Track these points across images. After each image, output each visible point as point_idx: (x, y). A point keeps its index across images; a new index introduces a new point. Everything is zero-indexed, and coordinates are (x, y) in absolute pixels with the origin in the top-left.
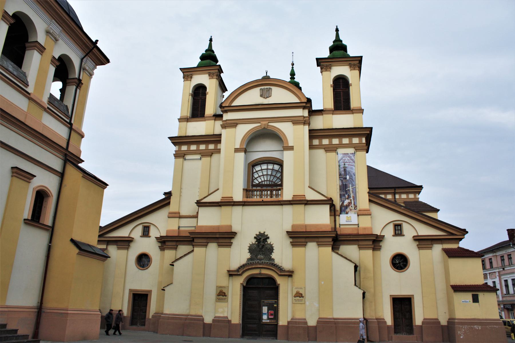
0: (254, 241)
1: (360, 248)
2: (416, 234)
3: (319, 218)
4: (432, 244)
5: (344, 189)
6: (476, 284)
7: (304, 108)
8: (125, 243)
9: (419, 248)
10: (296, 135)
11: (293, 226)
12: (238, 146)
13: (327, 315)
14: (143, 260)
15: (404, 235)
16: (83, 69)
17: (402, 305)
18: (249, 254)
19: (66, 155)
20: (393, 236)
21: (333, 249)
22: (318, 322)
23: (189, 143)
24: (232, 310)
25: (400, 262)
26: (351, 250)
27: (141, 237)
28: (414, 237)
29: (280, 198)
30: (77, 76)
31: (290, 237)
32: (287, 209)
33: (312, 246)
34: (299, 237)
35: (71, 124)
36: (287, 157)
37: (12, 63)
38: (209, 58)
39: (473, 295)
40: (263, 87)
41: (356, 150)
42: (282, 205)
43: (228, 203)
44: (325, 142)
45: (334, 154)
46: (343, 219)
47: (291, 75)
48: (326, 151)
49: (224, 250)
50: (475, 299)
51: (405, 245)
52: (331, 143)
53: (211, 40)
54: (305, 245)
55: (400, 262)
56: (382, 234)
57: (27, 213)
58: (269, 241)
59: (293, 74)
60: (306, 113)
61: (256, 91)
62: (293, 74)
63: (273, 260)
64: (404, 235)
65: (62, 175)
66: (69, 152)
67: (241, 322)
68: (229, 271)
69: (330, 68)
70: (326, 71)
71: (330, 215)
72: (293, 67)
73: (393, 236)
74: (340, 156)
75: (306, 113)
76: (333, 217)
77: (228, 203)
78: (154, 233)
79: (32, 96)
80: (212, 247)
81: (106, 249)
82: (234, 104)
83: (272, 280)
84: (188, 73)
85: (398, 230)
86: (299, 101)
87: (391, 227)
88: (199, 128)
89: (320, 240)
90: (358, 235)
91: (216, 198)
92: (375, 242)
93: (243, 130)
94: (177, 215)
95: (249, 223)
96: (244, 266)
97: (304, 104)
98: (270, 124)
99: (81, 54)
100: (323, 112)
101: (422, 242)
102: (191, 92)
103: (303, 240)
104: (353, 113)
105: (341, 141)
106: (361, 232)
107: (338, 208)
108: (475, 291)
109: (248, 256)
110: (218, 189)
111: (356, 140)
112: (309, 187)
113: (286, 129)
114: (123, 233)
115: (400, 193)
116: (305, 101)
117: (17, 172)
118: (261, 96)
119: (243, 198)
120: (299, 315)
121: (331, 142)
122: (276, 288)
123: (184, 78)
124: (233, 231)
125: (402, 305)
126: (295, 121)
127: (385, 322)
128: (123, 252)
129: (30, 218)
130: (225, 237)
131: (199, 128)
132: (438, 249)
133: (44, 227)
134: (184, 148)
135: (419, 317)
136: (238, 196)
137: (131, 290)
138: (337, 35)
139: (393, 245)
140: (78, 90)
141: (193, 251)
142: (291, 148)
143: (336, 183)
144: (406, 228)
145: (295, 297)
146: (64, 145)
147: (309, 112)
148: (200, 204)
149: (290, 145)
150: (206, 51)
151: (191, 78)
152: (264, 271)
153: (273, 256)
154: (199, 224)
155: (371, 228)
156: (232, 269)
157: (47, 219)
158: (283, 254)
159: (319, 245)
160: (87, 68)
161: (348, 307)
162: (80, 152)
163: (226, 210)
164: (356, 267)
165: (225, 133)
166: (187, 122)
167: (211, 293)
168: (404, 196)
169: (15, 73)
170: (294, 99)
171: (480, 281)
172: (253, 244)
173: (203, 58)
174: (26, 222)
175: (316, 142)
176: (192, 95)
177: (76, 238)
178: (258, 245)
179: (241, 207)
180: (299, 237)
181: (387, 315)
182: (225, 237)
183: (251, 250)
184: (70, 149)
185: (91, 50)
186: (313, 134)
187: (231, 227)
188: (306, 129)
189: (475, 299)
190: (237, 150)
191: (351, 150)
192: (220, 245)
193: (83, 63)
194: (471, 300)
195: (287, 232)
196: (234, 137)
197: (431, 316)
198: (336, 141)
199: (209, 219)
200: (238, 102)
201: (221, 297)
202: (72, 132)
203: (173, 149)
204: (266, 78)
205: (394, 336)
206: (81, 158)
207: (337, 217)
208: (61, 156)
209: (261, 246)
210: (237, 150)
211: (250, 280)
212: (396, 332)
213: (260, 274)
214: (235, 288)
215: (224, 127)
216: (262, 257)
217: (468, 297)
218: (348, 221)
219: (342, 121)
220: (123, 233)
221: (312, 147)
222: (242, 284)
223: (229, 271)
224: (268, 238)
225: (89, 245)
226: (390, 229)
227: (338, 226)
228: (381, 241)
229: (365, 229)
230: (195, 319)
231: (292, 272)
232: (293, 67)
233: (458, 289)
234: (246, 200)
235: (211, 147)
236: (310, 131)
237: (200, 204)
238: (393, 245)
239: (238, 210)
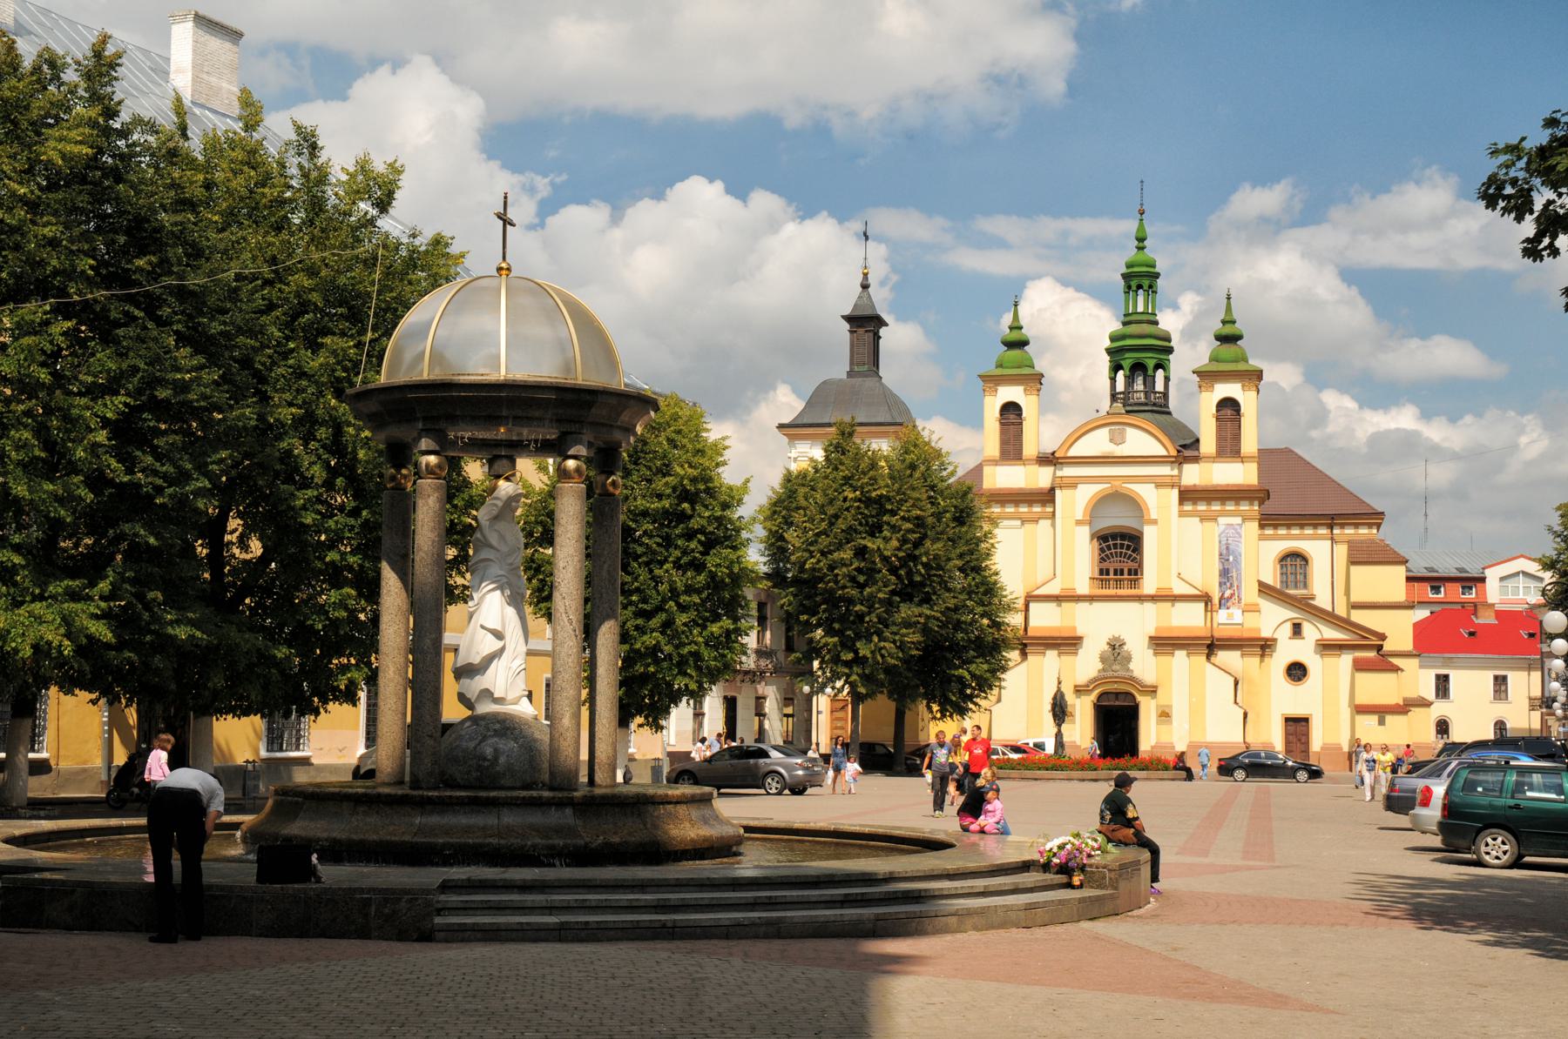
3: (1189, 618)
5: (1225, 573)
10: (1159, 502)
11: (1157, 629)
12: (1080, 517)
13: (1198, 738)
17: (1297, 726)
21: (1208, 657)
25: (1297, 671)
32: (1148, 606)
33: (1181, 655)
34: (1163, 643)
44: (1202, 507)
46: (1222, 616)
48: (1202, 520)
51: (1303, 650)
55: (1297, 671)
61: (1104, 433)
74: (1222, 528)
80: (1052, 654)
82: (1071, 453)
85: (1297, 630)
86: (1164, 453)
87: (1288, 626)
91: (1053, 589)
92: (1265, 647)
95: (1102, 623)
101: (1326, 647)
106: (1246, 635)
107: (1216, 600)
108: (1382, 712)
109: (1100, 666)
111: (1244, 507)
113: (1146, 492)
115: (1342, 526)
116: (1174, 453)
119: (1091, 587)
120: (1165, 739)
124: (1079, 634)
125: (1297, 726)
126: (1160, 483)
132: (1347, 659)
136: (1083, 588)
138: (1229, 309)
142: (1155, 522)
143: (1216, 567)
144: (1307, 628)
149: (1153, 516)
153: (1131, 666)
154: (1032, 623)
158: (1144, 665)
161: (1224, 730)
164: (1236, 683)
165: (1059, 495)
168: (1349, 531)
170: (1157, 449)
171: (1394, 699)
175: (1189, 507)
180: (1163, 643)
182: (1068, 643)
183: (1103, 659)
186: (1188, 495)
188: (1175, 492)
190: (1079, 523)
191: (1238, 520)
196: (1074, 503)
197: (1331, 740)
198: (1216, 507)
199: (1044, 618)
200: (1077, 450)
210: (1079, 523)
211: (1101, 696)
217: (1374, 718)
218: (1229, 619)
221: (1182, 514)
226: (1288, 628)
233: (1361, 710)
235: (1037, 509)
237: (1030, 598)
238: (1289, 650)
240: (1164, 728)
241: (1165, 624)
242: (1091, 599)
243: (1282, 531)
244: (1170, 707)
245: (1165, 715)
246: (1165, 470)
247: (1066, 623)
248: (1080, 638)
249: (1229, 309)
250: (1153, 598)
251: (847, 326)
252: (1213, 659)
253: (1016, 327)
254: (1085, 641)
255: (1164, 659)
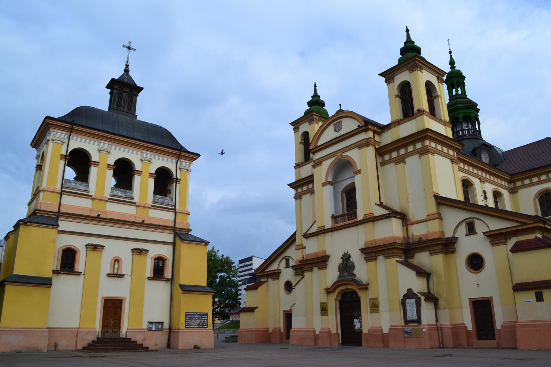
0: (341, 261)
1: (432, 254)
2: (488, 230)
4: (506, 239)
6: (545, 279)
7: (366, 130)
8: (276, 275)
9: (492, 244)
11: (365, 243)
14: (289, 287)
15: (476, 233)
16: (180, 169)
17: (482, 308)
18: (339, 273)
19: (174, 231)
20: (466, 235)
22: (390, 329)
23: (301, 186)
24: (332, 323)
25: (475, 262)
26: (422, 258)
27: (285, 268)
28: (484, 233)
29: (355, 220)
30: (175, 177)
31: (365, 254)
32: (361, 228)
34: (371, 252)
35: (175, 209)
36: (358, 179)
37: (122, 190)
38: (316, 103)
39: (536, 293)
40: (335, 123)
41: (420, 154)
42: (357, 225)
43: (323, 231)
44: (394, 155)
45: (402, 165)
47: (450, 64)
49: (322, 272)
50: (539, 298)
52: (399, 156)
53: (315, 86)
54: (375, 259)
55: (475, 262)
56: (456, 236)
57: (149, 272)
58: (351, 259)
59: (452, 63)
60: (370, 134)
62: (452, 63)
63: (355, 275)
64: (476, 233)
65: (174, 244)
66: (176, 228)
67: (339, 332)
68: (325, 289)
69: (393, 79)
70: (390, 83)
71: (403, 226)
72: (451, 56)
73: (466, 235)
75: (370, 134)
76: (405, 227)
77: (323, 231)
78: (292, 263)
79: (137, 204)
81: (267, 281)
83: (354, 294)
84: (296, 125)
88: (307, 170)
89: (386, 252)
90: (427, 241)
91: (314, 229)
92: (447, 246)
93: (326, 164)
94: (301, 247)
96: (335, 283)
97: (364, 128)
98: (344, 154)
99: (174, 160)
100: (390, 126)
101: (495, 238)
102: (300, 141)
103: (374, 255)
104: (415, 118)
105: (406, 150)
106: (430, 238)
108: (538, 288)
110: (315, 221)
111: (419, 145)
112: (381, 205)
113: (354, 154)
114: (274, 267)
116: (363, 124)
117: (136, 251)
118: (335, 130)
121: (398, 153)
122: (358, 300)
123: (294, 129)
125: (482, 308)
126: (360, 145)
127: (466, 328)
128: (276, 281)
129: (152, 276)
130: (321, 261)
131: (307, 170)
133: (167, 280)
134: (300, 190)
135: (499, 322)
136: (328, 224)
137: (284, 311)
139: (468, 245)
140: (178, 185)
141: (303, 276)
142: (359, 172)
145: (371, 307)
146: (172, 225)
147: (374, 132)
148: (307, 236)
150: (312, 97)
151: (298, 128)
152: (349, 287)
153: (355, 272)
155: (443, 233)
156: (329, 287)
157: (168, 274)
158: (362, 270)
159: (386, 257)
160: (182, 167)
162: (189, 225)
163: (321, 237)
166: (300, 167)
167: (317, 309)
169: (123, 195)
172: (341, 264)
173: (310, 104)
174: (149, 278)
175: (387, 157)
176: (301, 143)
177: (182, 283)
178: (343, 264)
179: (330, 233)
180: (371, 252)
181: (467, 320)
182: (321, 261)
184: (176, 226)
185: (180, 155)
186: (381, 152)
187: (325, 251)
189: (539, 298)
190: (324, 185)
192: (320, 269)
193: (178, 166)
194: (535, 300)
195: (360, 249)
196: (321, 173)
198: (402, 152)
199: (312, 247)
201: (323, 311)
202: (177, 214)
203: (293, 192)
204: (340, 111)
205: (475, 342)
206: (190, 228)
207: (409, 227)
208: (172, 232)
209: (346, 264)
210: (324, 185)
212: (480, 338)
213: (346, 289)
214: (332, 303)
215: (314, 167)
216: (346, 274)
217: (531, 296)
219: (408, 128)
220: (274, 267)
222: (336, 299)
223: (325, 289)
224: (350, 257)
225: (197, 286)
226: (463, 229)
227: (410, 235)
228: (455, 243)
229: (433, 233)
230: (307, 332)
231: (367, 285)
232: (451, 56)
233: (519, 288)
234: (333, 226)
236: (377, 150)
238: (468, 245)
239: (328, 236)
240: (375, 315)
241: (370, 239)
242: (332, 230)
243: (535, 180)
244: (376, 299)
245: (374, 306)
246: (363, 136)
247: (321, 249)
248: (329, 256)
249: (408, 36)
250: (362, 222)
251: (109, 91)
252: (410, 261)
253: (316, 96)
254: (330, 258)
255: (372, 263)
